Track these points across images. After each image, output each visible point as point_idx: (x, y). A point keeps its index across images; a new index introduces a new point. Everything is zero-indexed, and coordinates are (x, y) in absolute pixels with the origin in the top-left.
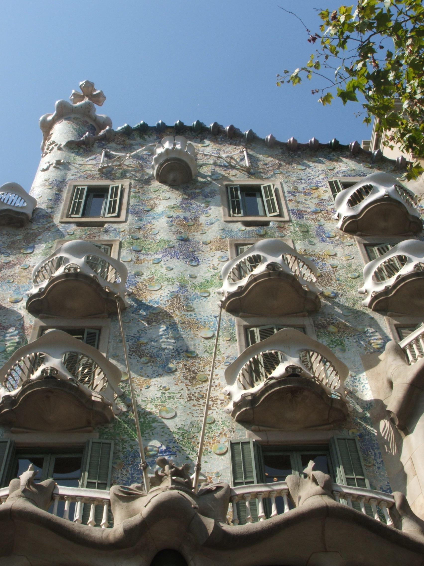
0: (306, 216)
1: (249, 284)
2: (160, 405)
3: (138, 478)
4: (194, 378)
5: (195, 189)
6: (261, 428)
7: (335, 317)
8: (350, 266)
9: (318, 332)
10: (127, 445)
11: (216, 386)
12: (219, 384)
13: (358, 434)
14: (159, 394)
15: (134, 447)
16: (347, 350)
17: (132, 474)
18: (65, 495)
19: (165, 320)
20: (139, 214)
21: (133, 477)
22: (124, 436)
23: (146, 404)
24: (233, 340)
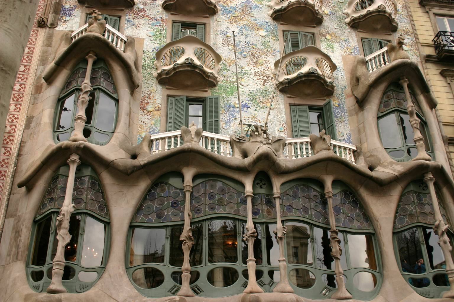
1: (288, 6)
2: (241, 78)
3: (232, 119)
4: (257, 62)
6: (292, 96)
7: (329, 29)
9: (321, 38)
10: (225, 100)
11: (268, 68)
12: (270, 66)
13: (338, 103)
15: (229, 102)
16: (335, 51)
17: (229, 117)
18: (208, 137)
19: (240, 22)
21: (230, 119)
22: (223, 95)
23: (233, 76)
24: (277, 39)
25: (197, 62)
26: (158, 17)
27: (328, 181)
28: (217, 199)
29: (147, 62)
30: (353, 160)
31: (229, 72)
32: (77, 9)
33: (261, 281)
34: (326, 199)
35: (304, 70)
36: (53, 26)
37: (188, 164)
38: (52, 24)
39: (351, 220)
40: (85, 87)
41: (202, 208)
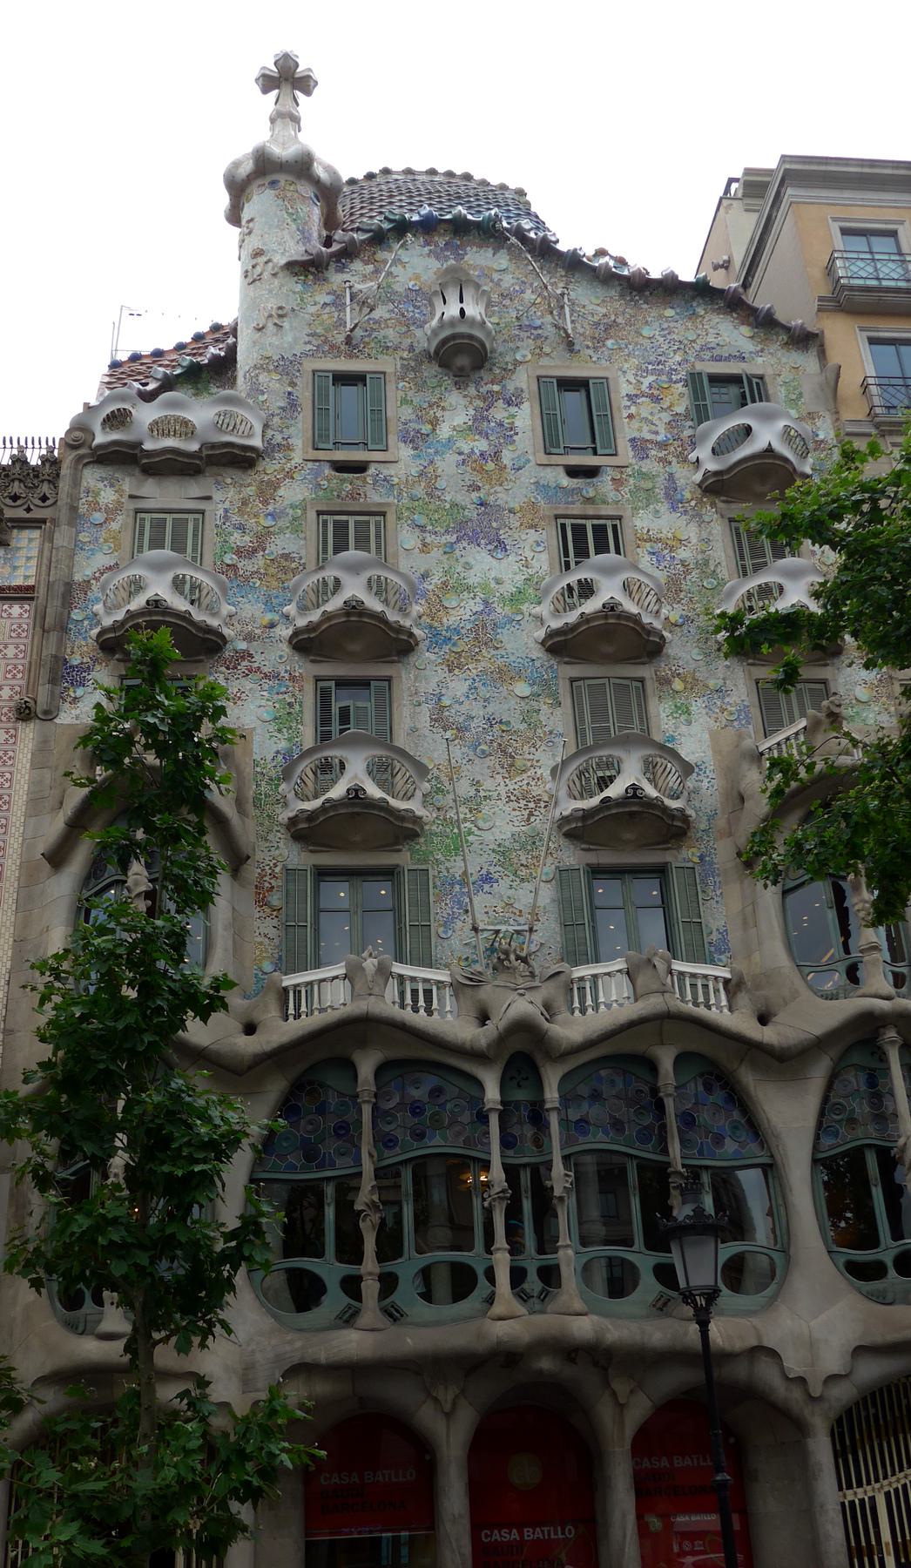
0: (653, 452)
4: (512, 765)
5: (493, 383)
8: (706, 563)
14: (472, 793)
20: (415, 439)
25: (374, 791)
26: (282, 669)
27: (666, 1059)
28: (428, 1114)
29: (264, 788)
30: (724, 1002)
31: (451, 797)
32: (98, 667)
33: (523, 1291)
34: (661, 1100)
35: (615, 790)
36: (49, 715)
37: (363, 1044)
38: (46, 712)
39: (719, 1140)
40: (137, 884)
41: (399, 1134)
